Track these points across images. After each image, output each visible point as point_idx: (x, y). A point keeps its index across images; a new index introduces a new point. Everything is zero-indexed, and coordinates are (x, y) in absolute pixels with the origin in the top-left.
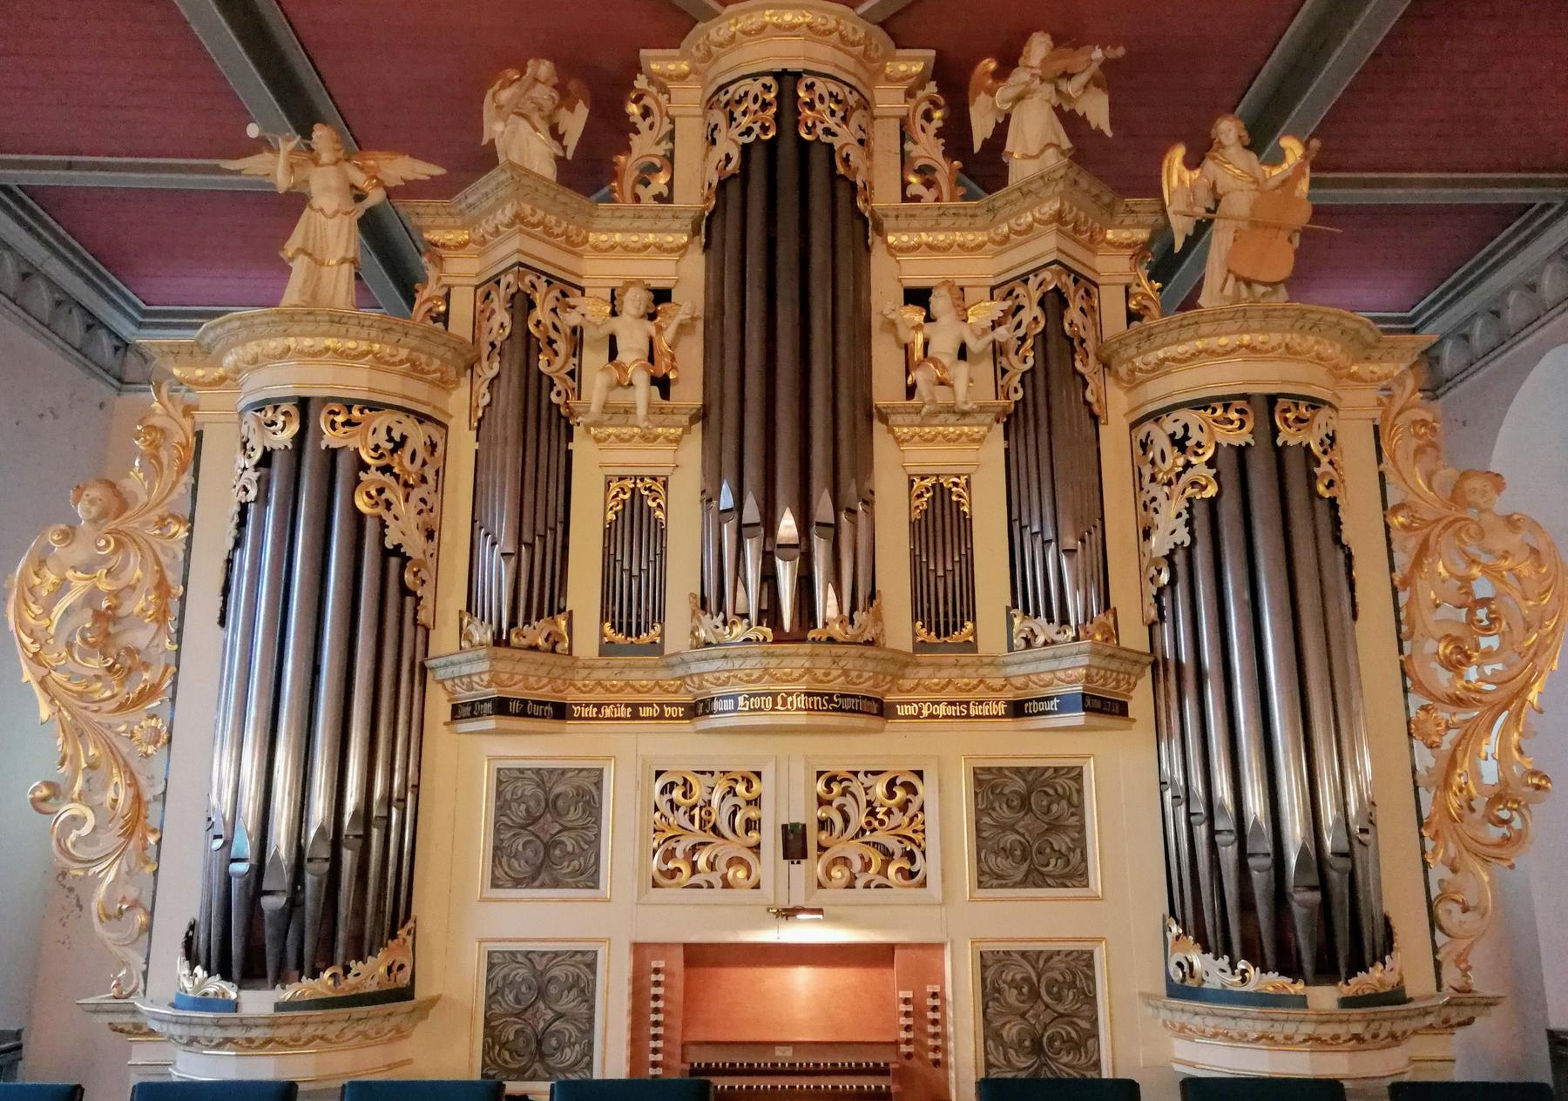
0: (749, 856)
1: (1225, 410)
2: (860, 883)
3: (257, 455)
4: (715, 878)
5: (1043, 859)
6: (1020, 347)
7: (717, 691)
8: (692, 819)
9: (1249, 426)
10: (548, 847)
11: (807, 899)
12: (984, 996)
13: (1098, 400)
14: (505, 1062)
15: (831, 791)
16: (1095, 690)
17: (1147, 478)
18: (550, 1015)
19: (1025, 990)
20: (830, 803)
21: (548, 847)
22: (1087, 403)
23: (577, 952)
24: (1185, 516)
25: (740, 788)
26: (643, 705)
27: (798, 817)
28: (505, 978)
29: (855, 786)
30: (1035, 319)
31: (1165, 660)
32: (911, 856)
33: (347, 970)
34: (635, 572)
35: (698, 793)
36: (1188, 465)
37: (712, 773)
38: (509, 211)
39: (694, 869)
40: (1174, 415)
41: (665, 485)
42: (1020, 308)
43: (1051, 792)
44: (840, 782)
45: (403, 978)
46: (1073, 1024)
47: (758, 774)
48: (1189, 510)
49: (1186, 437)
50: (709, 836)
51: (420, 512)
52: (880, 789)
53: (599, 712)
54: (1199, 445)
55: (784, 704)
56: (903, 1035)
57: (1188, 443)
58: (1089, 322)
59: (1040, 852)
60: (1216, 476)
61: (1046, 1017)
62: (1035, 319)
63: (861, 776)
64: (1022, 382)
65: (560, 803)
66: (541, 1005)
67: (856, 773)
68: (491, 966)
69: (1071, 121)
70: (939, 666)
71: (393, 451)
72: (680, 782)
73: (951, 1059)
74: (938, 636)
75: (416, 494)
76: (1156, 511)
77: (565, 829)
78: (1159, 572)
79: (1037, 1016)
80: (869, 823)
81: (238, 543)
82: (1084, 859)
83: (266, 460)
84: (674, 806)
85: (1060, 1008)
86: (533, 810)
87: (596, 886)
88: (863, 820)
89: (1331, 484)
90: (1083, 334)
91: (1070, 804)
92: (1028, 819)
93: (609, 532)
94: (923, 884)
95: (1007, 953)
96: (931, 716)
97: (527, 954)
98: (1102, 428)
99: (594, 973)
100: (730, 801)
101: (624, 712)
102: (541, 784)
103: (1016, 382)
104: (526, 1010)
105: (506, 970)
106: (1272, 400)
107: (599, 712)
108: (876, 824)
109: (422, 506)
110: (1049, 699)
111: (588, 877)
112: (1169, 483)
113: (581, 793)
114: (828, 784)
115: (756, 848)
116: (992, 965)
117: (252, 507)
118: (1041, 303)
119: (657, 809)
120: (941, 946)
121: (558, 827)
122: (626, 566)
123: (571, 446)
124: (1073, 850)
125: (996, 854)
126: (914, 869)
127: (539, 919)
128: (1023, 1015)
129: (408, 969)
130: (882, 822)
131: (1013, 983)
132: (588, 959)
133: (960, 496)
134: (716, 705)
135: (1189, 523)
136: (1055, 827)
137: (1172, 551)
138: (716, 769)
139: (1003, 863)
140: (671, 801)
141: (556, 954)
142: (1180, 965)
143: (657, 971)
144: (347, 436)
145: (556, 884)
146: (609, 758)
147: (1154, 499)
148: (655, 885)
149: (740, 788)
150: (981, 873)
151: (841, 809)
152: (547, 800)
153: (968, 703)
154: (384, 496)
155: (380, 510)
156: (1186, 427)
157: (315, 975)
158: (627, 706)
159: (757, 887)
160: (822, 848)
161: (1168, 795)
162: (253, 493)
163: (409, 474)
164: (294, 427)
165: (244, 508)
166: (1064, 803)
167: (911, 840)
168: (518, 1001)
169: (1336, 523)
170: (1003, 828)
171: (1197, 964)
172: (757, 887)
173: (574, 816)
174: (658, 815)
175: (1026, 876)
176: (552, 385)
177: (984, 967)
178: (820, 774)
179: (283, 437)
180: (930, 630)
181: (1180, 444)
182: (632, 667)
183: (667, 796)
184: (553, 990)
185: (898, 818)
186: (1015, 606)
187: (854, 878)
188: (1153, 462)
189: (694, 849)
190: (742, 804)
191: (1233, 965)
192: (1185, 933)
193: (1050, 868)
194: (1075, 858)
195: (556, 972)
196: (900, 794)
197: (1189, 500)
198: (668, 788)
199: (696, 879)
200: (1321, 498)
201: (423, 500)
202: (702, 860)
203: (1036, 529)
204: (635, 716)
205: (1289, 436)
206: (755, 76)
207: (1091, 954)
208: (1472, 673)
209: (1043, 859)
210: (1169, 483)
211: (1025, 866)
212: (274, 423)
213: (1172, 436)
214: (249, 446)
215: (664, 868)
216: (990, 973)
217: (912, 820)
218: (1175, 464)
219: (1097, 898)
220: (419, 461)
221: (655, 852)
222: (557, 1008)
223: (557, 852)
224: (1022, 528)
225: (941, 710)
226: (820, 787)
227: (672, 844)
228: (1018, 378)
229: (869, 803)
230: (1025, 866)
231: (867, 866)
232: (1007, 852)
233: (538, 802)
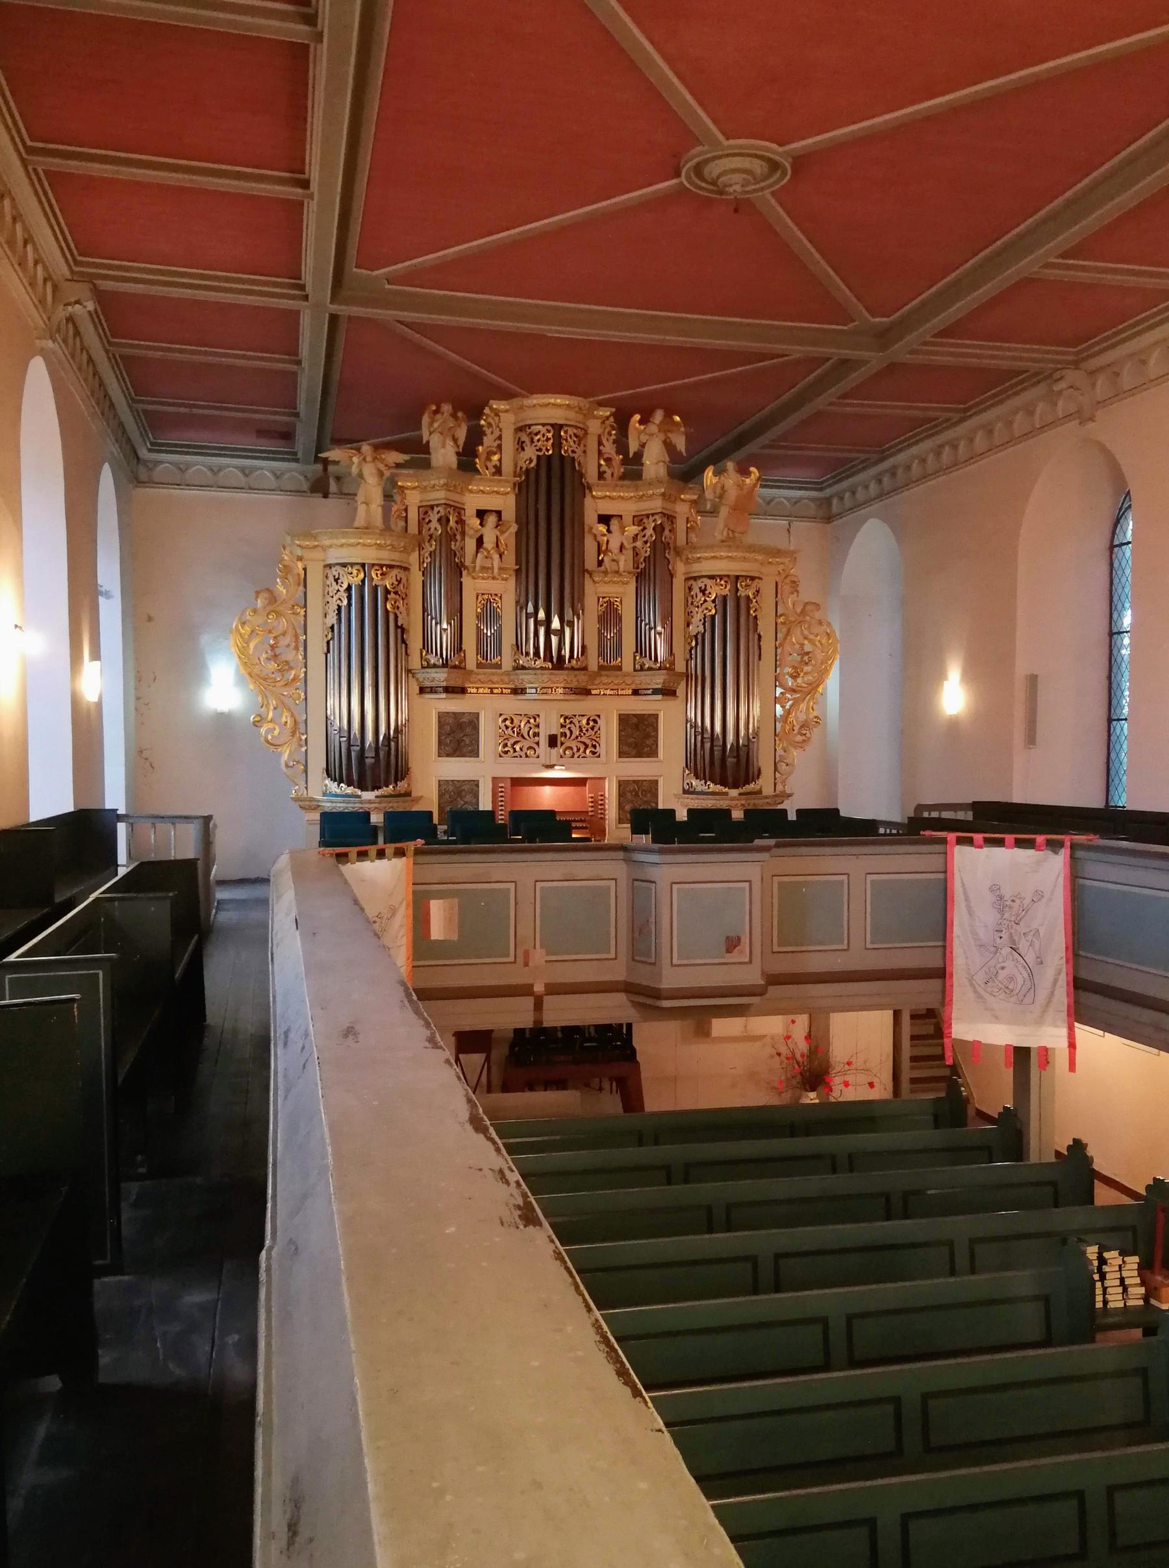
0: (535, 746)
27: (554, 732)
29: (575, 720)
32: (594, 747)
36: (705, 601)
38: (442, 482)
39: (515, 751)
52: (584, 722)
69: (669, 446)
83: (349, 589)
84: (507, 727)
106: (737, 577)
111: (475, 753)
115: (538, 744)
116: (622, 785)
120: (603, 779)
127: (457, 769)
131: (631, 792)
136: (648, 736)
149: (532, 721)
160: (562, 744)
173: (468, 730)
181: (703, 591)
185: (591, 732)
194: (654, 747)
196: (591, 723)
198: (505, 720)
202: (517, 747)
204: (492, 693)
206: (544, 425)
208: (799, 680)
225: (608, 692)
226: (562, 720)
231: (578, 750)
232: (629, 745)
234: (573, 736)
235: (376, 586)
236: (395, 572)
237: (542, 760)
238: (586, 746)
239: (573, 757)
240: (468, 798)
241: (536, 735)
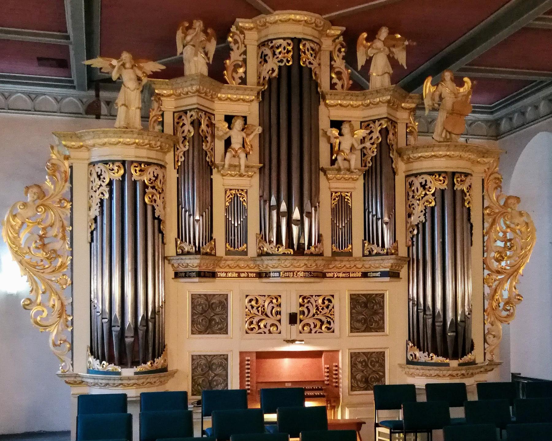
0: (278, 324)
1: (439, 177)
2: (313, 331)
4: (266, 330)
7: (272, 270)
9: (446, 182)
18: (213, 375)
19: (364, 364)
20: (303, 306)
22: (392, 167)
24: (424, 212)
29: (312, 300)
30: (378, 137)
32: (329, 323)
35: (261, 302)
36: (426, 194)
37: (265, 296)
41: (246, 193)
46: (378, 374)
47: (280, 296)
48: (425, 210)
49: (426, 185)
52: (320, 301)
59: (370, 321)
63: (314, 297)
67: (312, 296)
73: (341, 385)
76: (414, 209)
77: (216, 314)
78: (414, 230)
80: (316, 312)
82: (384, 323)
84: (252, 307)
88: (315, 311)
89: (469, 203)
91: (380, 306)
94: (333, 332)
95: (359, 353)
100: (271, 305)
101: (235, 275)
102: (207, 300)
103: (369, 159)
106: (454, 174)
110: (378, 272)
111: (224, 330)
113: (221, 302)
114: (303, 300)
115: (279, 321)
116: (354, 356)
123: (212, 177)
126: (330, 327)
128: (363, 371)
130: (320, 312)
132: (225, 357)
133: (348, 200)
134: (272, 274)
135: (425, 215)
136: (376, 313)
139: (358, 325)
142: (411, 355)
145: (214, 333)
147: (413, 204)
150: (351, 328)
151: (307, 307)
153: (349, 273)
156: (426, 181)
157: (145, 363)
166: (378, 305)
167: (330, 318)
171: (417, 355)
174: (247, 310)
177: (351, 357)
178: (300, 296)
181: (424, 186)
183: (250, 304)
184: (214, 367)
187: (311, 330)
188: (413, 191)
190: (275, 306)
192: (414, 346)
197: (425, 206)
198: (251, 301)
199: (260, 331)
200: (466, 207)
203: (374, 213)
210: (419, 200)
213: (421, 183)
215: (250, 327)
218: (421, 194)
223: (213, 322)
224: (369, 213)
226: (301, 300)
229: (316, 306)
230: (365, 326)
231: (315, 326)
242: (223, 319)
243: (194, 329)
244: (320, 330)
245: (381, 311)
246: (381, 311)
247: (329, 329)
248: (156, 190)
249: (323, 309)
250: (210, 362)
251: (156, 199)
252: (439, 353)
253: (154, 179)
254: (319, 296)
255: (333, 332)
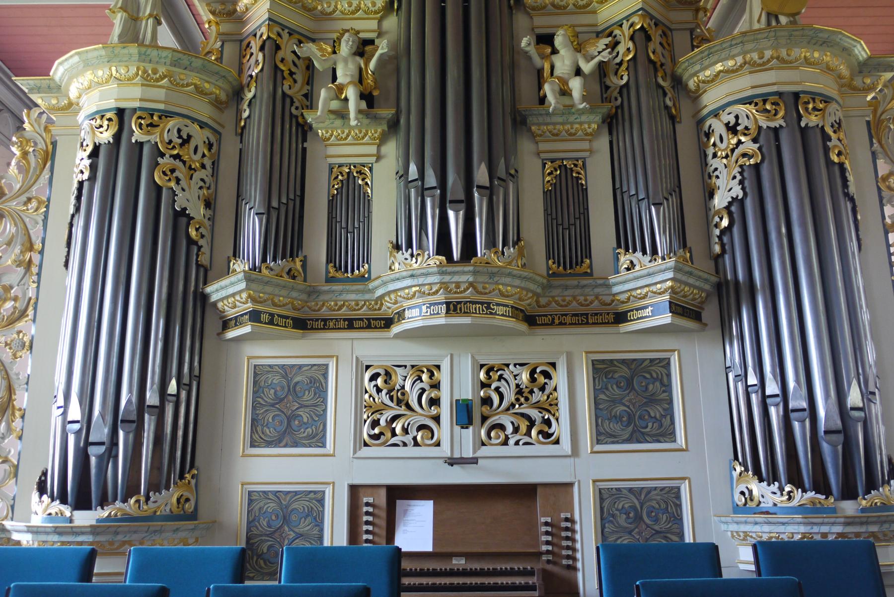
1: (764, 104)
2: (512, 442)
3: (89, 149)
4: (408, 439)
5: (643, 424)
6: (618, 70)
7: (406, 304)
8: (391, 398)
9: (781, 114)
10: (290, 419)
11: (474, 452)
12: (602, 519)
13: (674, 105)
14: (261, 567)
15: (490, 377)
16: (678, 300)
17: (710, 156)
18: (292, 535)
19: (631, 515)
20: (489, 386)
21: (290, 419)
22: (667, 107)
23: (311, 492)
24: (739, 177)
25: (425, 377)
26: (356, 319)
28: (260, 509)
29: (507, 374)
30: (628, 49)
31: (727, 281)
32: (548, 423)
33: (148, 498)
34: (350, 229)
35: (397, 380)
36: (740, 142)
37: (405, 366)
39: (394, 434)
40: (728, 110)
41: (371, 169)
42: (617, 43)
43: (648, 376)
44: (497, 371)
45: (189, 507)
46: (666, 538)
47: (438, 367)
48: (741, 173)
49: (737, 124)
50: (402, 410)
51: (201, 188)
52: (525, 377)
53: (325, 325)
54: (746, 128)
55: (455, 310)
56: (544, 548)
57: (739, 128)
58: (666, 53)
59: (641, 418)
60: (760, 149)
61: (646, 534)
62: (628, 49)
63: (511, 367)
64: (620, 93)
65: (298, 388)
66: (286, 528)
67: (508, 365)
68: (251, 501)
70: (566, 288)
71: (182, 145)
72: (382, 372)
73: (579, 565)
74: (565, 268)
75: (197, 175)
76: (717, 177)
78: (721, 219)
79: (640, 533)
80: (517, 400)
81: (77, 209)
82: (673, 422)
84: (379, 390)
85: (657, 527)
86: (279, 393)
87: (324, 446)
88: (513, 399)
89: (839, 154)
90: (663, 61)
91: (662, 384)
92: (632, 396)
93: (332, 203)
94: (557, 442)
95: (618, 490)
96: (561, 324)
97: (276, 493)
98: (677, 126)
99: (323, 506)
100: (419, 385)
102: (285, 376)
103: (616, 94)
104: (275, 532)
105: (262, 504)
106: (796, 95)
107: (325, 325)
108: (522, 400)
109: (202, 184)
110: (646, 307)
111: (318, 439)
112: (727, 157)
113: (313, 381)
114: (487, 373)
115: (437, 419)
116: (608, 498)
117: (86, 184)
118: (632, 38)
119: (366, 392)
120: (570, 485)
121: (297, 405)
122: (344, 225)
123: (305, 145)
124: (665, 416)
125: (610, 419)
126: (551, 431)
128: (630, 533)
129: (193, 502)
130: (527, 399)
132: (319, 496)
133: (579, 173)
134: (407, 314)
135: (741, 182)
136: (652, 400)
137: (730, 204)
138: (408, 364)
139: (615, 427)
140: (376, 386)
141: (296, 493)
142: (742, 493)
143: (367, 504)
144: (149, 133)
145: (296, 445)
146: (332, 357)
147: (716, 169)
148: (366, 445)
149: (425, 377)
150: (599, 433)
151: (497, 389)
152: (289, 386)
153: (587, 315)
154: (174, 175)
155: (173, 184)
156: (737, 117)
158: (345, 320)
159: (438, 444)
160: (484, 419)
161: (731, 376)
162: (86, 176)
163: (194, 161)
164: (114, 129)
165: (81, 183)
166: (658, 384)
167: (549, 411)
168: (269, 526)
169: (845, 181)
170: (614, 402)
171: (755, 493)
172: (438, 444)
173: (307, 397)
174: (367, 396)
175: (632, 435)
176: (292, 102)
177: (602, 500)
178: (482, 366)
179: (106, 136)
180: (559, 265)
181: (732, 129)
182: (348, 292)
183: (374, 383)
184: (293, 518)
186: (619, 246)
187: (507, 438)
188: (714, 145)
189: (395, 418)
190: (427, 387)
191: (781, 489)
192: (747, 470)
193: (648, 430)
194: (666, 422)
195: (295, 506)
196: (542, 380)
197: (741, 166)
198: (374, 378)
199: (394, 440)
200: (835, 163)
201: (202, 180)
203: (633, 192)
205: (811, 120)
207: (679, 488)
209: (643, 424)
210: (727, 157)
211: (630, 428)
212: (101, 126)
213: (727, 125)
214: (85, 144)
215: (372, 432)
216: (606, 504)
217: (548, 397)
218: (729, 143)
219: (682, 450)
220: (200, 154)
221: (365, 421)
222: (297, 530)
223: (297, 422)
224: (622, 193)
226: (482, 375)
227: (376, 416)
228: (618, 90)
229: (518, 386)
230: (630, 428)
231: (516, 430)
232: (618, 419)
233: (283, 388)
234: (505, 404)
235: (141, 145)
236: (172, 123)
237: (445, 450)
238: (532, 423)
239: (505, 443)
240: (305, 527)
241: (435, 402)
242: (317, 416)
243: (256, 437)
244: (527, 439)
245: (664, 396)
246: (664, 396)
247: (548, 436)
248: (184, 162)
249: (531, 392)
250: (287, 507)
251: (181, 176)
252: (807, 486)
253: (180, 141)
254: (521, 365)
255: (557, 442)
